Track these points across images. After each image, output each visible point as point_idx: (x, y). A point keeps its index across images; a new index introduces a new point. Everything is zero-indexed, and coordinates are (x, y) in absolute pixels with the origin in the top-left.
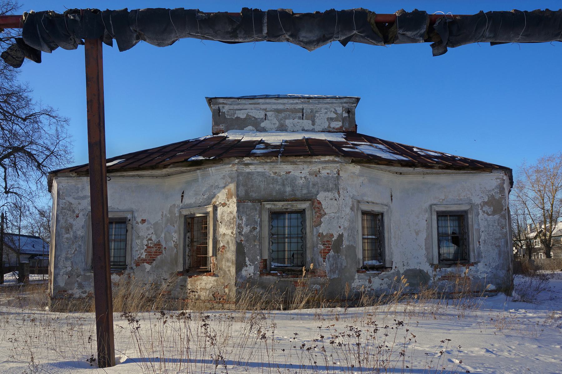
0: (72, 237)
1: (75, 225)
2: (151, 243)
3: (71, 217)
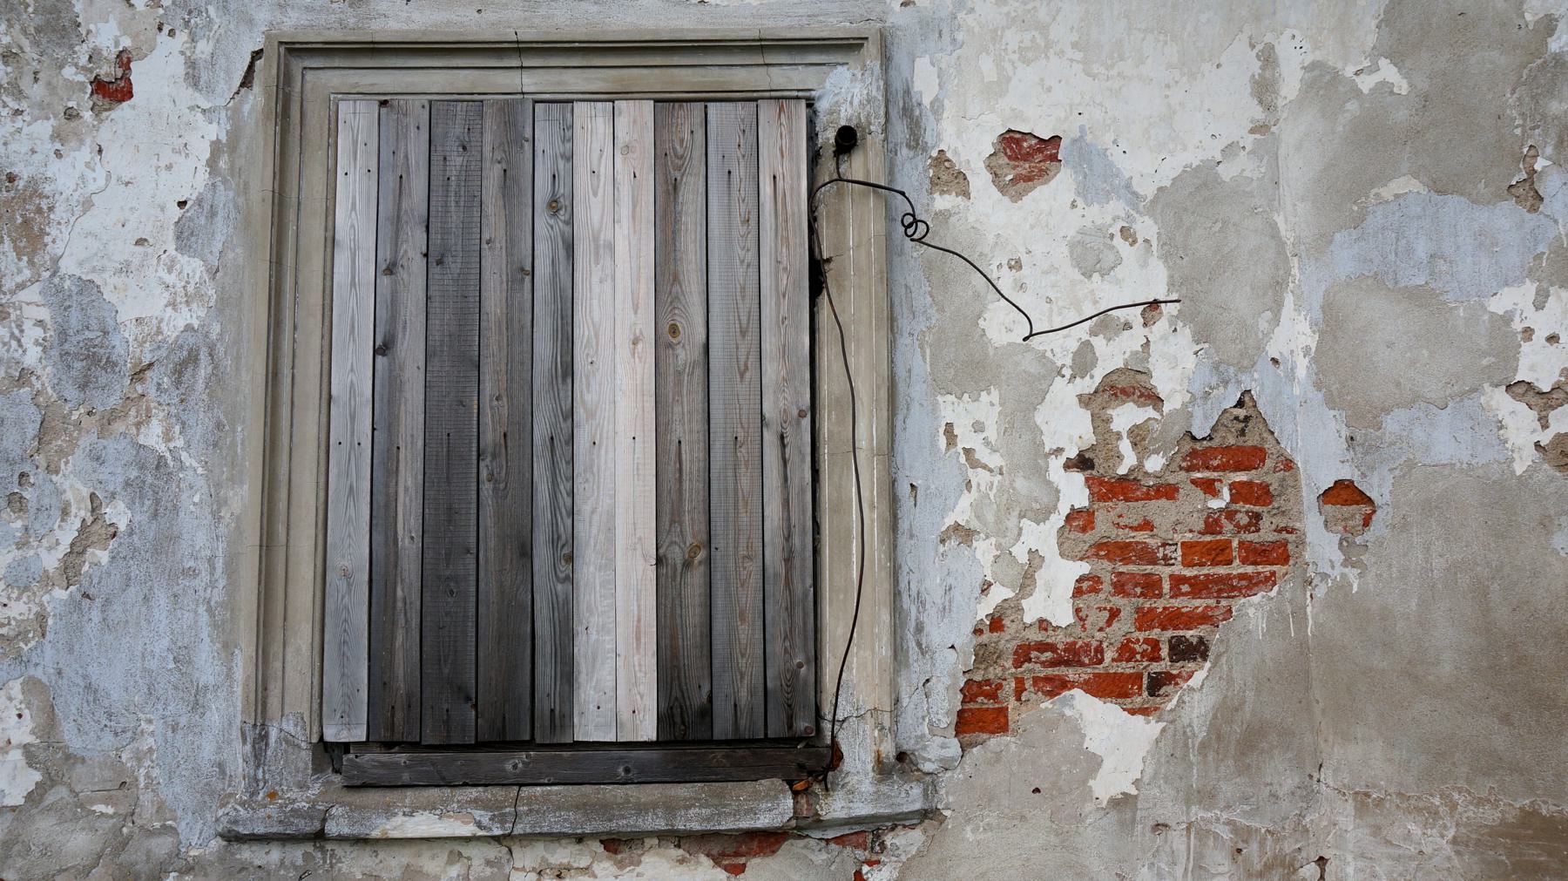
0: (32, 356)
1: (87, 204)
2: (1138, 436)
3: (19, 94)
